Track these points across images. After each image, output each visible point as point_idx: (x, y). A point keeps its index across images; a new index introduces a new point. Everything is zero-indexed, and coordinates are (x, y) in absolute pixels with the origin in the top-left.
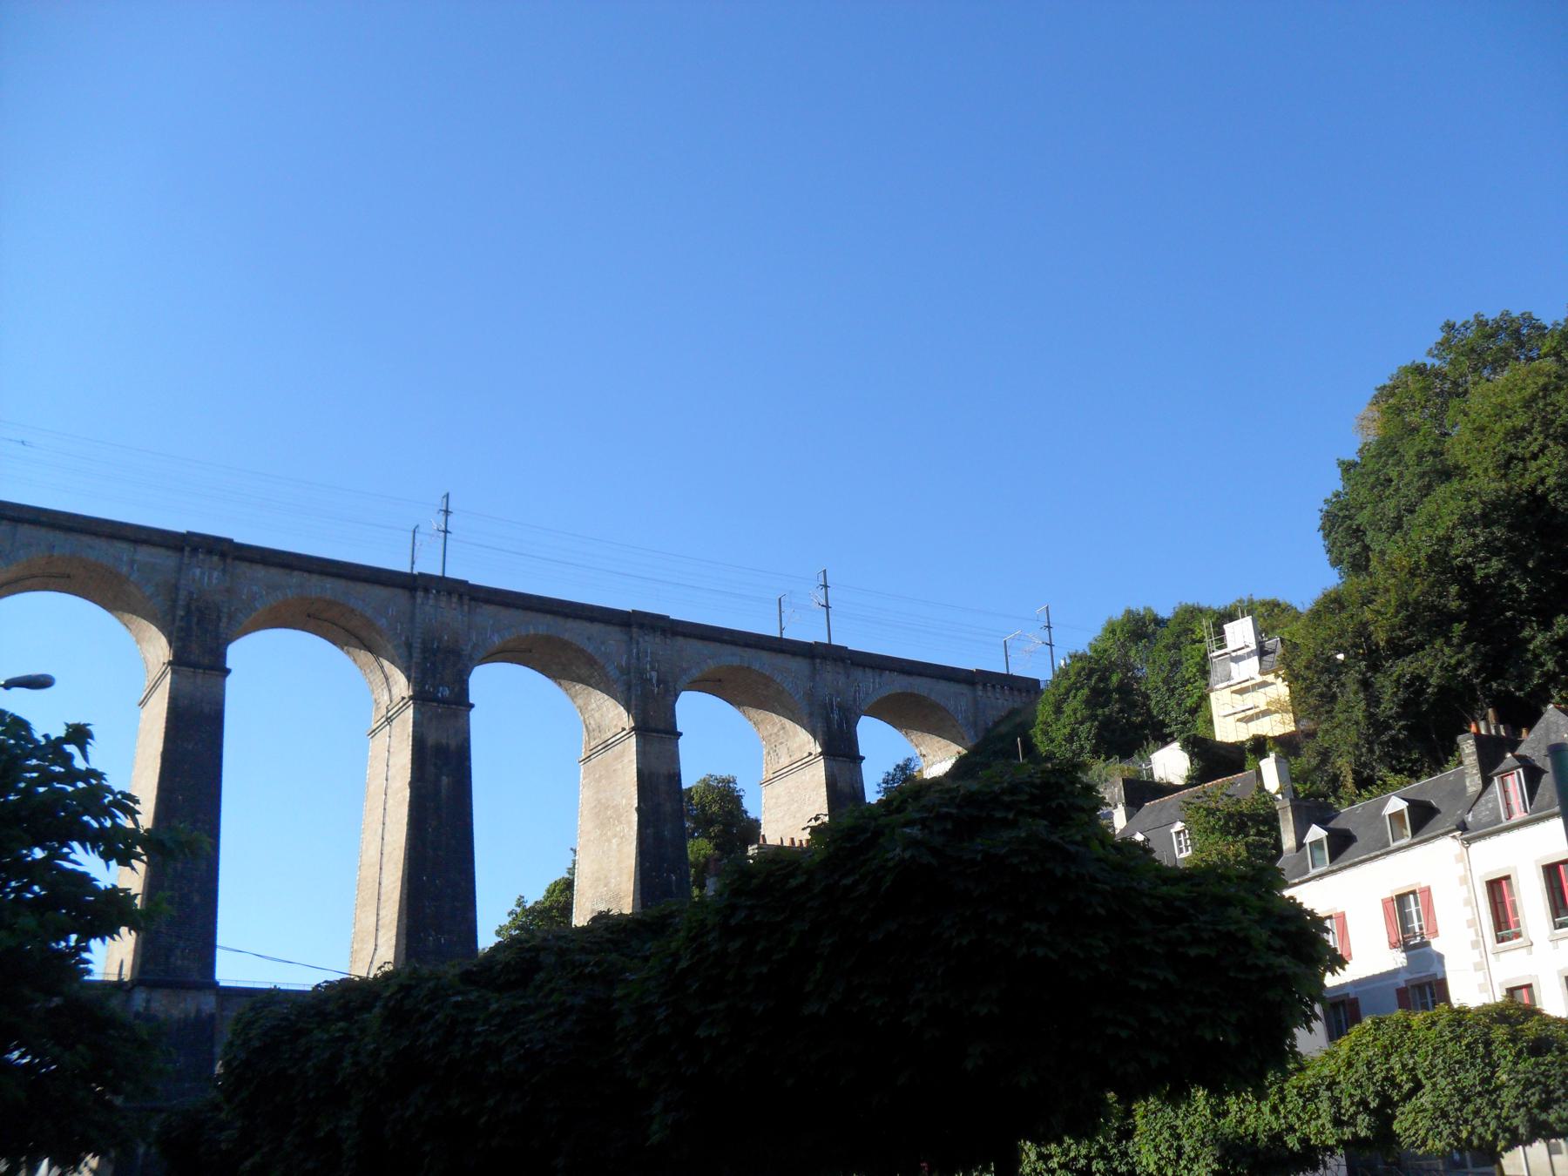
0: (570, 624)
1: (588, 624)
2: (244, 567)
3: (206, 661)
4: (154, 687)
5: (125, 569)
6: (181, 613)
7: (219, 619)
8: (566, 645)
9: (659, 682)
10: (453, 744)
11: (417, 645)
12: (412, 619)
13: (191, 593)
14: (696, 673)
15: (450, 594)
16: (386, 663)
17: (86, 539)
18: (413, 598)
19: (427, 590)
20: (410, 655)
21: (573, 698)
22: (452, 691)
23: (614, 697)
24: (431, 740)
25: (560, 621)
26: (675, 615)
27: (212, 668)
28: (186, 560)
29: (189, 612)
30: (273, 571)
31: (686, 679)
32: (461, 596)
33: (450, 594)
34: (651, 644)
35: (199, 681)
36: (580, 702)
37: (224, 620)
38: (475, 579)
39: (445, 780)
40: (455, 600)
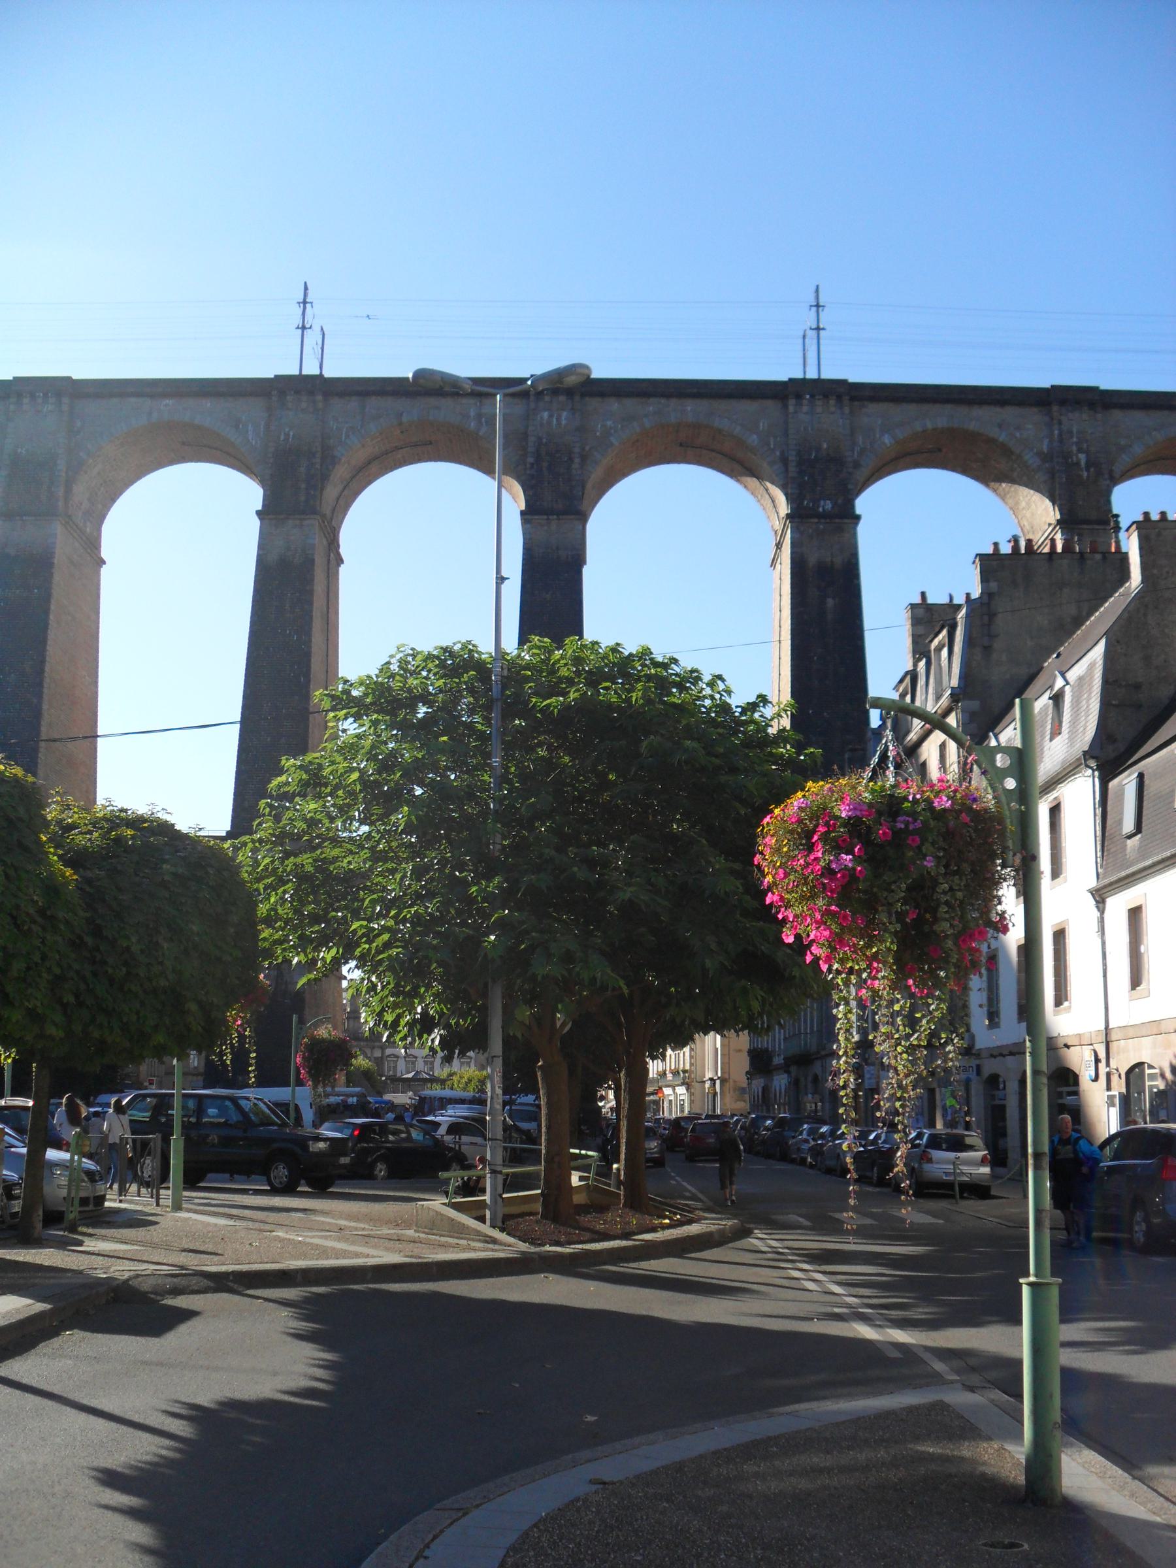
1: (998, 409)
2: (594, 403)
4: (779, 546)
6: (530, 460)
7: (571, 459)
8: (972, 438)
10: (838, 561)
11: (792, 457)
12: (786, 433)
13: (540, 439)
14: (1138, 450)
15: (826, 396)
16: (768, 484)
17: (432, 401)
18: (785, 407)
19: (799, 397)
20: (787, 470)
22: (835, 504)
23: (1038, 490)
26: (1106, 384)
28: (532, 405)
30: (630, 404)
31: (1125, 460)
32: (839, 398)
33: (826, 396)
34: (1077, 422)
36: (1010, 501)
37: (577, 460)
38: (855, 376)
39: (830, 602)
40: (832, 402)
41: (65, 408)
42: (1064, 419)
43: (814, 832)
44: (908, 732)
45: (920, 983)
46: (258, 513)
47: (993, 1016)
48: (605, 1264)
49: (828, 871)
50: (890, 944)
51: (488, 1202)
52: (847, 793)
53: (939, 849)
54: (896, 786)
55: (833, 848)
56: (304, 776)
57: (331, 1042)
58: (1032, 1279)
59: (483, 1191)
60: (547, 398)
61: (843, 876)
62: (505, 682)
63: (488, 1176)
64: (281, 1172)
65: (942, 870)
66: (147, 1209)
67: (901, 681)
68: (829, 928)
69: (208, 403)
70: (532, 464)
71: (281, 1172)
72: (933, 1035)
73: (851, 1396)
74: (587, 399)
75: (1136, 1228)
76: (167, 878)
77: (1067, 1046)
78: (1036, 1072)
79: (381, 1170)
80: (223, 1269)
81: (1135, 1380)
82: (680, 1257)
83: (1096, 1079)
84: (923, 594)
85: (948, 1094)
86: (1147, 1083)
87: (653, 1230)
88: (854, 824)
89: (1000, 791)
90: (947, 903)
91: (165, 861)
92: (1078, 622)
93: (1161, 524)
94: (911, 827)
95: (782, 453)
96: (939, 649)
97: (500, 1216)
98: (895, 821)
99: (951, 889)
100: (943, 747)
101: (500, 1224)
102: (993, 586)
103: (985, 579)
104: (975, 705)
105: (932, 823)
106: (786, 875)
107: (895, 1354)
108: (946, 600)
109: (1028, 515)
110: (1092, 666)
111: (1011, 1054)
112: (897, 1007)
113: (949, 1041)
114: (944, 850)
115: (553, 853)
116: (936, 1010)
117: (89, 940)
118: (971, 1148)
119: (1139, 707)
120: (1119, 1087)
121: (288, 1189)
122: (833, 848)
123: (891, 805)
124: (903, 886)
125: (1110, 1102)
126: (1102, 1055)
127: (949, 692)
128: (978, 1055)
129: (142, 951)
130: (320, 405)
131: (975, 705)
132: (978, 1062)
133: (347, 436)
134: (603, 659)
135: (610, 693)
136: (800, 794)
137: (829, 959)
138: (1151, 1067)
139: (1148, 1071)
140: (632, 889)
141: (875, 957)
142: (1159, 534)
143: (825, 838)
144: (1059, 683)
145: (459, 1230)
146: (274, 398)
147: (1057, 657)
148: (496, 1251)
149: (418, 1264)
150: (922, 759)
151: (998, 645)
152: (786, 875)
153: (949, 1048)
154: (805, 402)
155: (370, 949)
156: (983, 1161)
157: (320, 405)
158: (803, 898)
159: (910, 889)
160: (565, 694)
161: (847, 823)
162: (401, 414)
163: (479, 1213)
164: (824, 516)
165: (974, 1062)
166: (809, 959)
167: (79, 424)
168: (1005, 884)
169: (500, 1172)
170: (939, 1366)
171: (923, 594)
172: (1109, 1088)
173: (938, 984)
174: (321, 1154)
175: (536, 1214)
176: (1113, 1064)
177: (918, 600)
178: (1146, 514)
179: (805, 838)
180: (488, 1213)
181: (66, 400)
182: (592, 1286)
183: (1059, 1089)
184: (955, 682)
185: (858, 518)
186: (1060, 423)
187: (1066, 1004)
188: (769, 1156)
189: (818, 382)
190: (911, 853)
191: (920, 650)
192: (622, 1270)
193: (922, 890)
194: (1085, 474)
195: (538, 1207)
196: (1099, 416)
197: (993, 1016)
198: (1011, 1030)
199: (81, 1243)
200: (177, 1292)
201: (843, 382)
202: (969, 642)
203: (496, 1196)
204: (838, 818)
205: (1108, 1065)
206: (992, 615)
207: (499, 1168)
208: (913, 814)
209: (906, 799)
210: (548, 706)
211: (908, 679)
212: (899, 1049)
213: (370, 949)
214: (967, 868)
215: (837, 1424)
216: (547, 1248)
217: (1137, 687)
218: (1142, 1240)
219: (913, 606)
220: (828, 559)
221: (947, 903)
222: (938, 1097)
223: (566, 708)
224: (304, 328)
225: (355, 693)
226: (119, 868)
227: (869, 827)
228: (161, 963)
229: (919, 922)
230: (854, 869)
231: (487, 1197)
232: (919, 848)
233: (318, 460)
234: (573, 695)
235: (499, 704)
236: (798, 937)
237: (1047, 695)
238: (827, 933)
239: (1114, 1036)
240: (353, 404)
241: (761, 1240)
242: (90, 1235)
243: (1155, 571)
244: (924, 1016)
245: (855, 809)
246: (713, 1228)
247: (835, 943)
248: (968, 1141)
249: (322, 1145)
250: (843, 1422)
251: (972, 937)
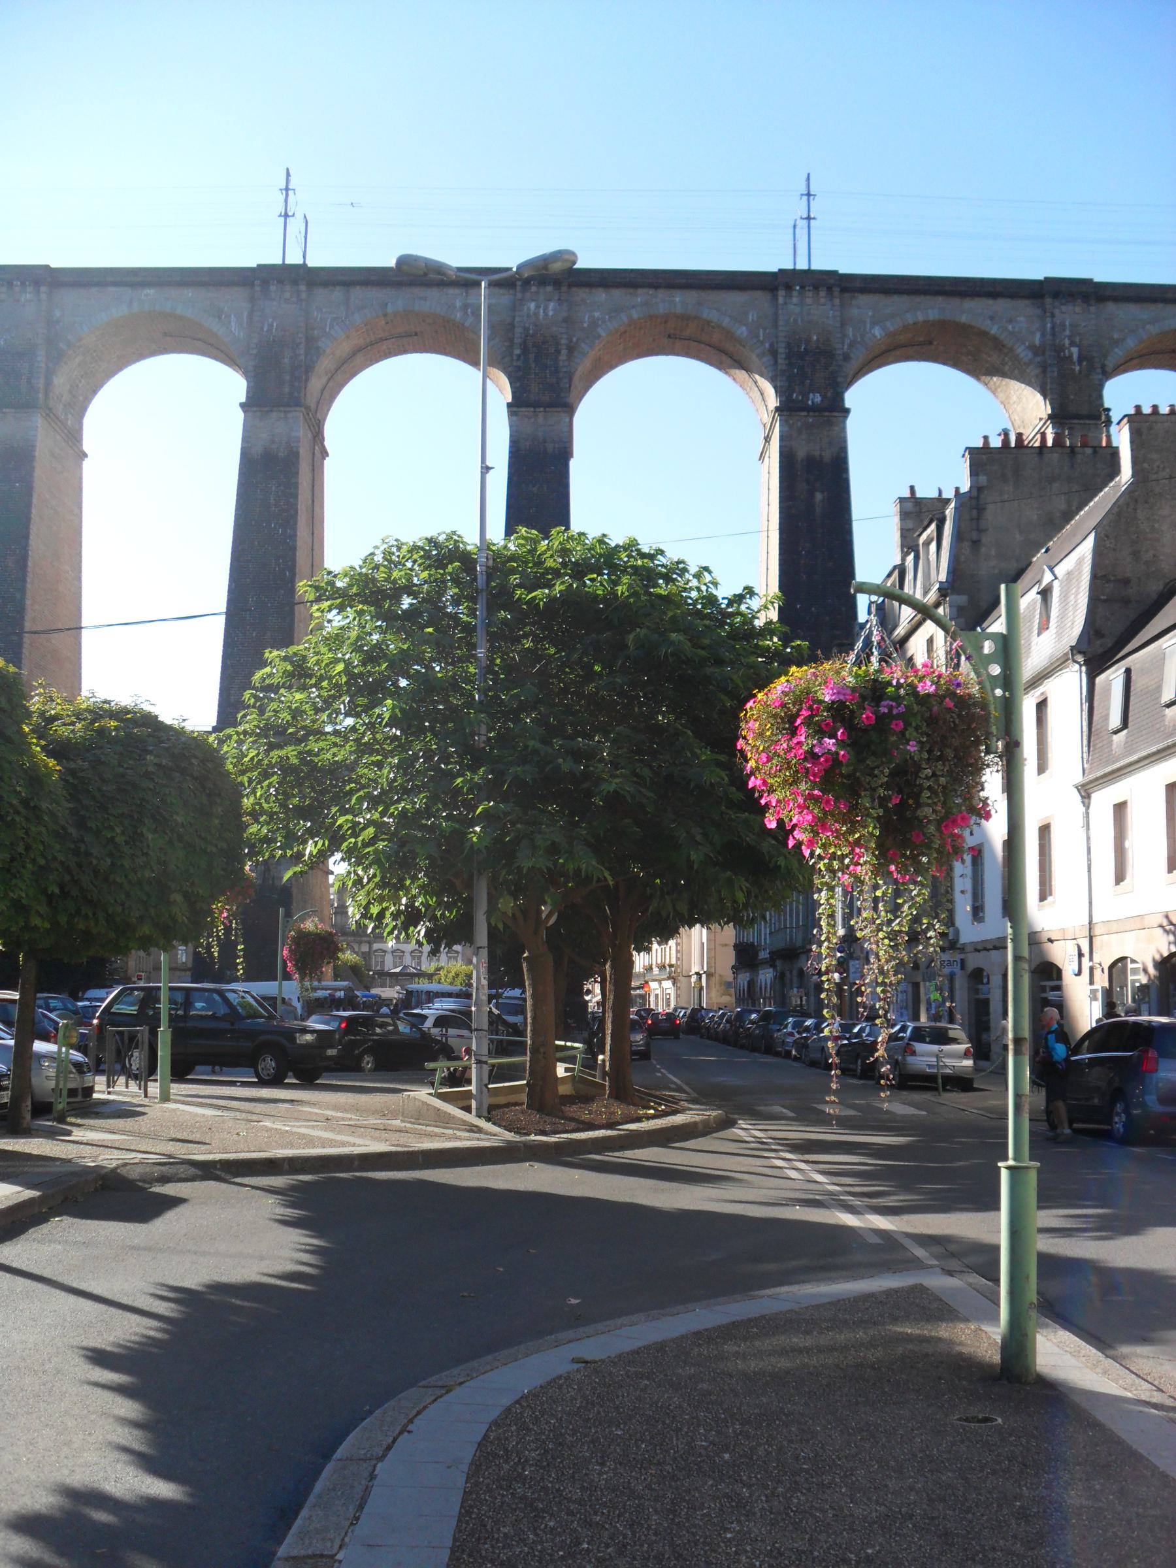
0: (969, 304)
1: (991, 302)
2: (581, 294)
3: (546, 398)
4: (767, 439)
6: (517, 352)
7: (558, 352)
8: (964, 330)
9: (1081, 359)
10: (827, 455)
12: (776, 325)
13: (526, 329)
14: (1131, 343)
15: (816, 288)
16: (757, 377)
17: (417, 291)
18: (775, 298)
19: (789, 288)
20: (776, 362)
21: (994, 392)
22: (824, 397)
23: (1029, 384)
24: (801, 454)
25: (955, 302)
27: (551, 405)
28: (519, 296)
29: (525, 350)
30: (616, 293)
31: (1118, 353)
32: (829, 289)
33: (816, 288)
34: (1069, 314)
35: (540, 419)
36: (1002, 395)
37: (564, 352)
38: (846, 267)
39: (819, 496)
40: (822, 293)
41: (43, 296)
42: (1057, 312)
43: (798, 715)
44: (895, 626)
45: (903, 869)
46: (242, 405)
47: (978, 912)
48: (590, 1153)
49: (811, 756)
50: (873, 829)
51: (474, 1092)
52: (831, 678)
53: (922, 734)
54: (880, 671)
55: (816, 732)
56: (289, 668)
57: (317, 935)
58: (1011, 1162)
59: (469, 1082)
60: (534, 289)
61: (826, 760)
62: (490, 575)
63: (474, 1066)
64: (269, 1064)
65: (926, 755)
66: (135, 1101)
67: (889, 576)
68: (812, 812)
69: (189, 293)
70: (519, 356)
71: (269, 1064)
72: (916, 920)
73: (832, 1280)
74: (574, 289)
75: (1116, 1119)
76: (151, 769)
77: (1051, 941)
78: (1017, 958)
79: (368, 1062)
80: (210, 1157)
81: (1111, 1265)
82: (664, 1145)
83: (1079, 973)
84: (912, 488)
85: (932, 988)
86: (1130, 978)
87: (638, 1120)
88: (838, 710)
89: (984, 677)
90: (929, 788)
91: (151, 752)
92: (1068, 516)
93: (1152, 418)
94: (895, 712)
95: (772, 345)
96: (927, 543)
97: (485, 1107)
98: (878, 705)
99: (934, 775)
100: (930, 641)
101: (485, 1114)
102: (983, 479)
103: (974, 473)
104: (962, 599)
105: (916, 708)
106: (769, 759)
107: (876, 1240)
108: (935, 495)
109: (1019, 409)
110: (1080, 561)
111: (995, 948)
112: (879, 893)
113: (931, 926)
114: (928, 735)
115: (538, 745)
116: (918, 895)
117: (73, 831)
118: (954, 1041)
119: (1126, 601)
120: (1102, 981)
121: (276, 1081)
122: (816, 732)
123: (875, 690)
124: (887, 771)
125: (1093, 996)
126: (1086, 950)
127: (937, 586)
128: (962, 949)
129: (127, 843)
130: (304, 295)
131: (962, 599)
132: (962, 956)
133: (331, 327)
134: (589, 550)
135: (596, 584)
136: (783, 679)
137: (811, 843)
138: (1133, 961)
139: (1130, 966)
140: (617, 780)
141: (857, 843)
142: (1150, 428)
143: (808, 722)
144: (1048, 577)
145: (444, 1120)
146: (258, 288)
147: (1046, 551)
148: (482, 1140)
149: (408, 1152)
150: (909, 654)
151: (986, 539)
152: (769, 759)
153: (931, 934)
154: (795, 293)
155: (356, 842)
156: (966, 1054)
157: (304, 295)
158: (785, 783)
159: (891, 775)
160: (550, 586)
161: (830, 707)
163: (465, 1103)
164: (815, 409)
165: (958, 957)
166: (791, 843)
167: (58, 313)
168: (988, 770)
169: (486, 1063)
170: (919, 1252)
171: (912, 488)
172: (1092, 982)
173: (920, 869)
174: (307, 1046)
175: (522, 1104)
176: (1097, 958)
177: (907, 494)
178: (1138, 408)
179: (788, 723)
180: (474, 1103)
182: (577, 1174)
183: (1044, 983)
184: (943, 577)
185: (847, 411)
186: (1053, 315)
187: (1050, 899)
188: (753, 1049)
189: (809, 272)
190: (895, 738)
191: (909, 544)
192: (606, 1158)
193: (905, 777)
194: (1077, 368)
195: (524, 1098)
196: (1093, 309)
197: (978, 912)
198: (995, 925)
199: (69, 1133)
200: (165, 1179)
201: (833, 274)
202: (958, 536)
203: (482, 1086)
204: (821, 702)
205: (1091, 959)
206: (980, 509)
207: (484, 1059)
208: (897, 698)
209: (889, 684)
210: (534, 598)
211: (896, 573)
212: (881, 935)
213: (356, 842)
214: (950, 753)
215: (818, 1307)
216: (533, 1137)
217: (1126, 582)
218: (1122, 1130)
219: (902, 500)
220: (817, 453)
221: (929, 788)
222: (922, 990)
223: (552, 600)
224: (286, 216)
225: (339, 584)
226: (103, 758)
227: (852, 712)
228: (146, 854)
229: (902, 807)
230: (837, 753)
231: (473, 1088)
232: (903, 733)
233: (302, 351)
234: (558, 588)
235: (484, 594)
236: (780, 822)
237: (1036, 589)
238: (810, 817)
239: (1097, 931)
240: (337, 294)
241: (745, 1129)
242: (79, 1125)
243: (1146, 465)
244: (905, 902)
245: (838, 693)
246: (698, 1118)
247: (818, 826)
248: (952, 1034)
249: (309, 1037)
250: (825, 1304)
251: (954, 823)
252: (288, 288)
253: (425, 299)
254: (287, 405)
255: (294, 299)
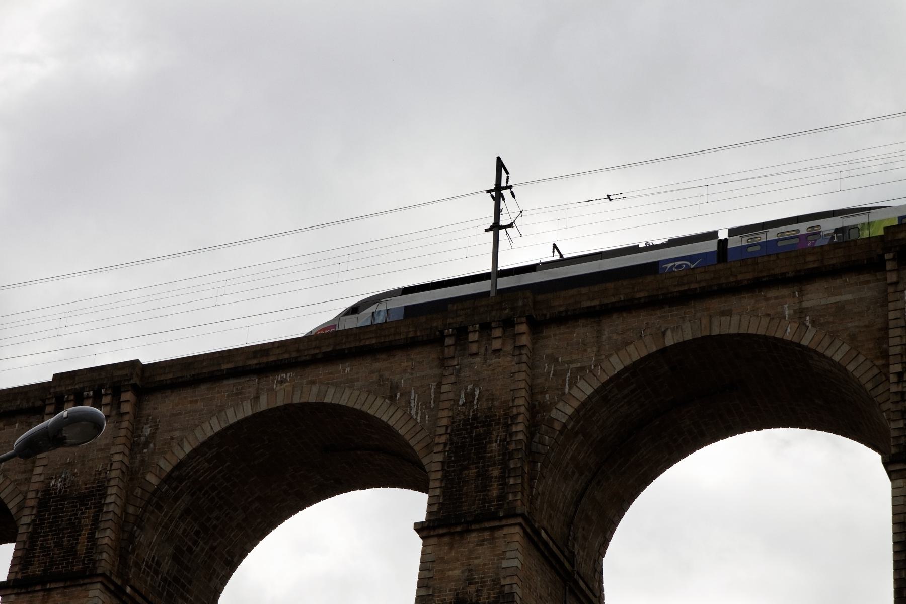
5: (789, 332)
17: (716, 304)
28: (892, 277)
46: (419, 528)
69: (345, 369)
130: (525, 340)
162: (664, 333)
167: (147, 431)
181: (128, 396)
240: (583, 332)
252: (497, 332)
253: (728, 313)
254: (494, 517)
255: (509, 348)
